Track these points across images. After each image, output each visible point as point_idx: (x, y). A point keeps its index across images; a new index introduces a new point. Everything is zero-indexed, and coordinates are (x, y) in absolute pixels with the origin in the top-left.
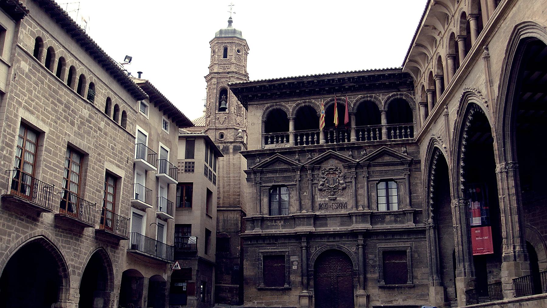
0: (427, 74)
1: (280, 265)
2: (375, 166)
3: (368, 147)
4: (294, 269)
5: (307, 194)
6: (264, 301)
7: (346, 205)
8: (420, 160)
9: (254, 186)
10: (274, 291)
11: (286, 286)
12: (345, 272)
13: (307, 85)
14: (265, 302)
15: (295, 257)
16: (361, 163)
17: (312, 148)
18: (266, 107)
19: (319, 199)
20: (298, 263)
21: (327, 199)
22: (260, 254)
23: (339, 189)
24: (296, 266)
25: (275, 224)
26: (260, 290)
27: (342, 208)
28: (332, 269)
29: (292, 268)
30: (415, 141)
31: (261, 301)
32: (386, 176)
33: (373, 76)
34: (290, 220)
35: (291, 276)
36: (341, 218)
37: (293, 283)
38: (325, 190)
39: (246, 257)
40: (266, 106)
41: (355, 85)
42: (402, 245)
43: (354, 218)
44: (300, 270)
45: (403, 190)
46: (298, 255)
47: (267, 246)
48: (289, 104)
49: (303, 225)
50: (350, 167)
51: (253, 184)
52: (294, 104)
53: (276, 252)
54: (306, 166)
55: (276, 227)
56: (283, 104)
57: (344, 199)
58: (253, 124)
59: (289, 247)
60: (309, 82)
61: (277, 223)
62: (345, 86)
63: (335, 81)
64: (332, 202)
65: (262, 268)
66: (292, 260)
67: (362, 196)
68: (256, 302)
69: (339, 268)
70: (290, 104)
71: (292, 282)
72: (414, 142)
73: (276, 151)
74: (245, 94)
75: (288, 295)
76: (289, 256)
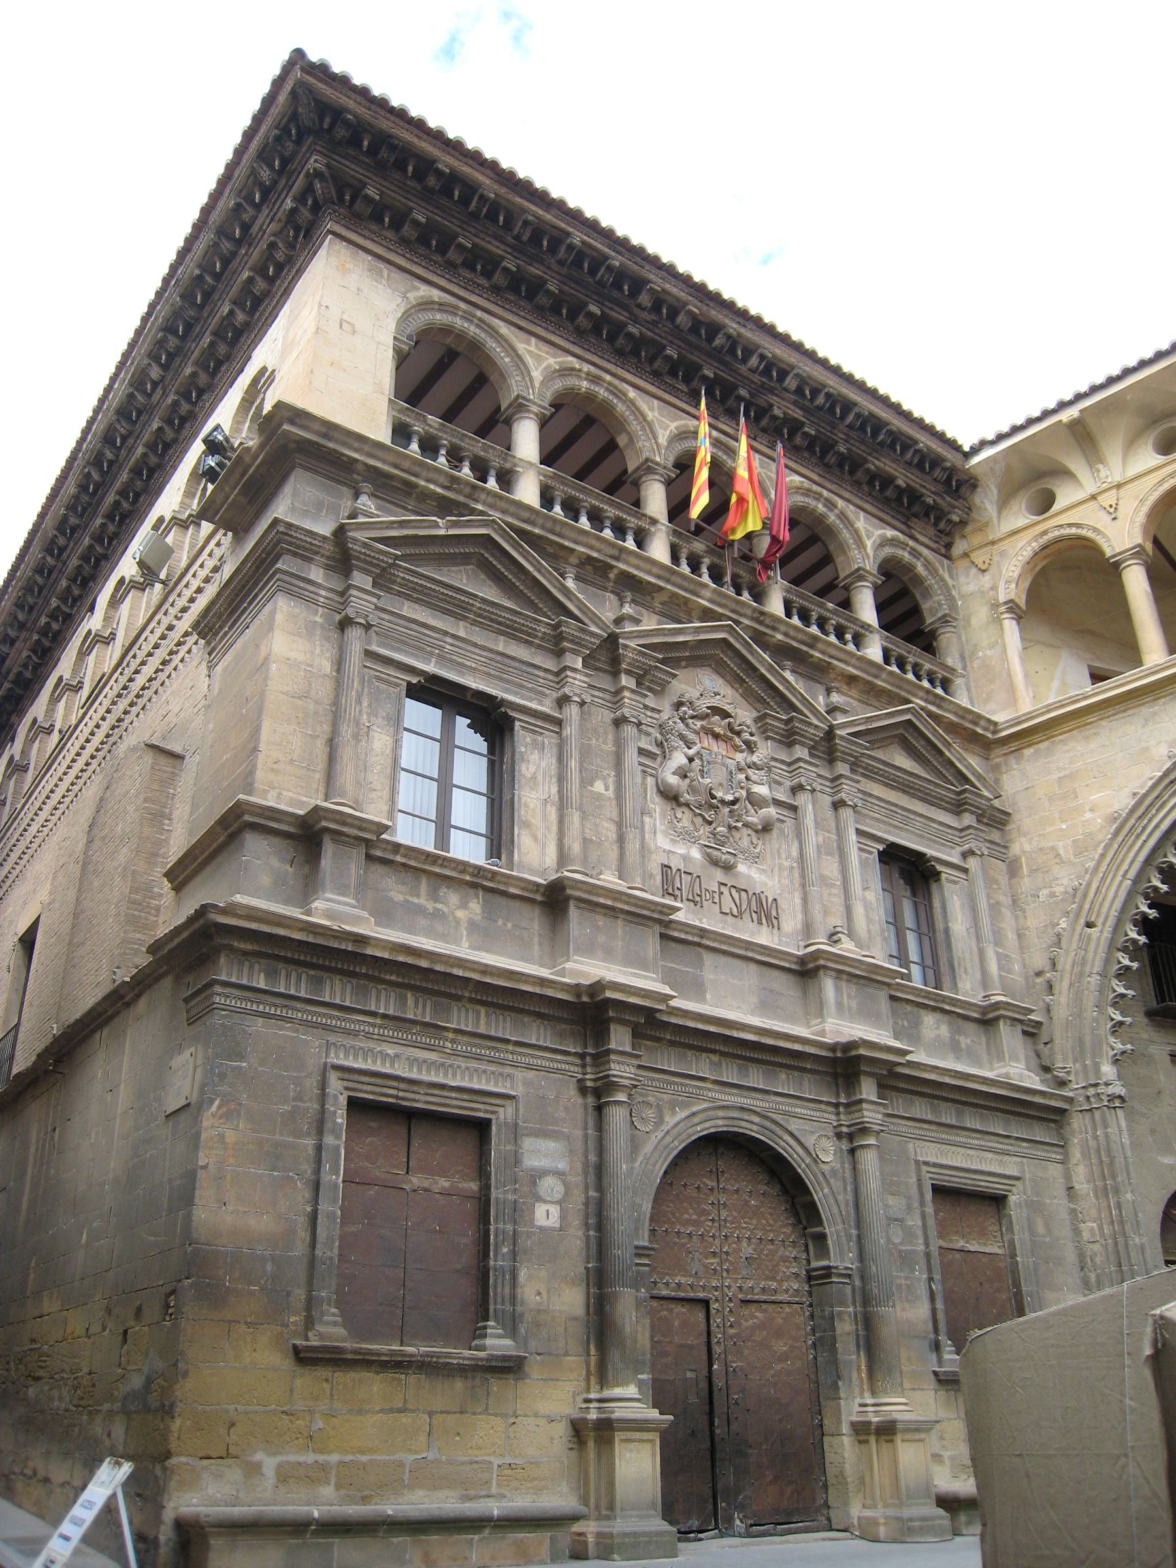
0: (1153, 490)
1: (444, 1183)
2: (871, 774)
3: (845, 688)
4: (541, 1228)
5: (611, 793)
6: (334, 1458)
7: (774, 913)
8: (1008, 814)
9: (319, 632)
10: (412, 1379)
11: (497, 1343)
12: (773, 1279)
13: (644, 309)
14: (342, 1463)
15: (551, 1145)
16: (842, 738)
17: (649, 573)
18: (422, 293)
19: (663, 842)
20: (566, 1185)
21: (696, 854)
22: (335, 1084)
23: (746, 825)
24: (555, 1210)
25: (430, 906)
26: (304, 1358)
27: (760, 923)
28: (714, 1254)
29: (532, 1220)
30: (994, 733)
31: (310, 1458)
32: (903, 834)
33: (878, 425)
34: (517, 904)
35: (523, 1274)
36: (765, 969)
37: (538, 1325)
38: (687, 805)
39: (225, 1088)
40: (424, 291)
41: (803, 424)
42: (990, 1163)
43: (829, 986)
44: (576, 1241)
45: (959, 916)
46: (567, 1137)
47: (382, 1040)
48: (529, 344)
49: (609, 954)
50: (788, 739)
51: (318, 619)
52: (552, 361)
53: (442, 1087)
54: (626, 647)
55: (439, 927)
56: (504, 329)
57: (764, 878)
58: (345, 325)
59: (519, 1074)
60: (659, 302)
61: (446, 903)
62: (771, 406)
63: (754, 361)
64: (719, 875)
65: (336, 1185)
66: (532, 1161)
67: (835, 891)
68: (270, 1464)
69: (747, 1250)
70: (533, 349)
71: (528, 1318)
72: (990, 736)
73: (480, 507)
74: (353, 170)
75: (504, 1416)
76: (515, 1132)
